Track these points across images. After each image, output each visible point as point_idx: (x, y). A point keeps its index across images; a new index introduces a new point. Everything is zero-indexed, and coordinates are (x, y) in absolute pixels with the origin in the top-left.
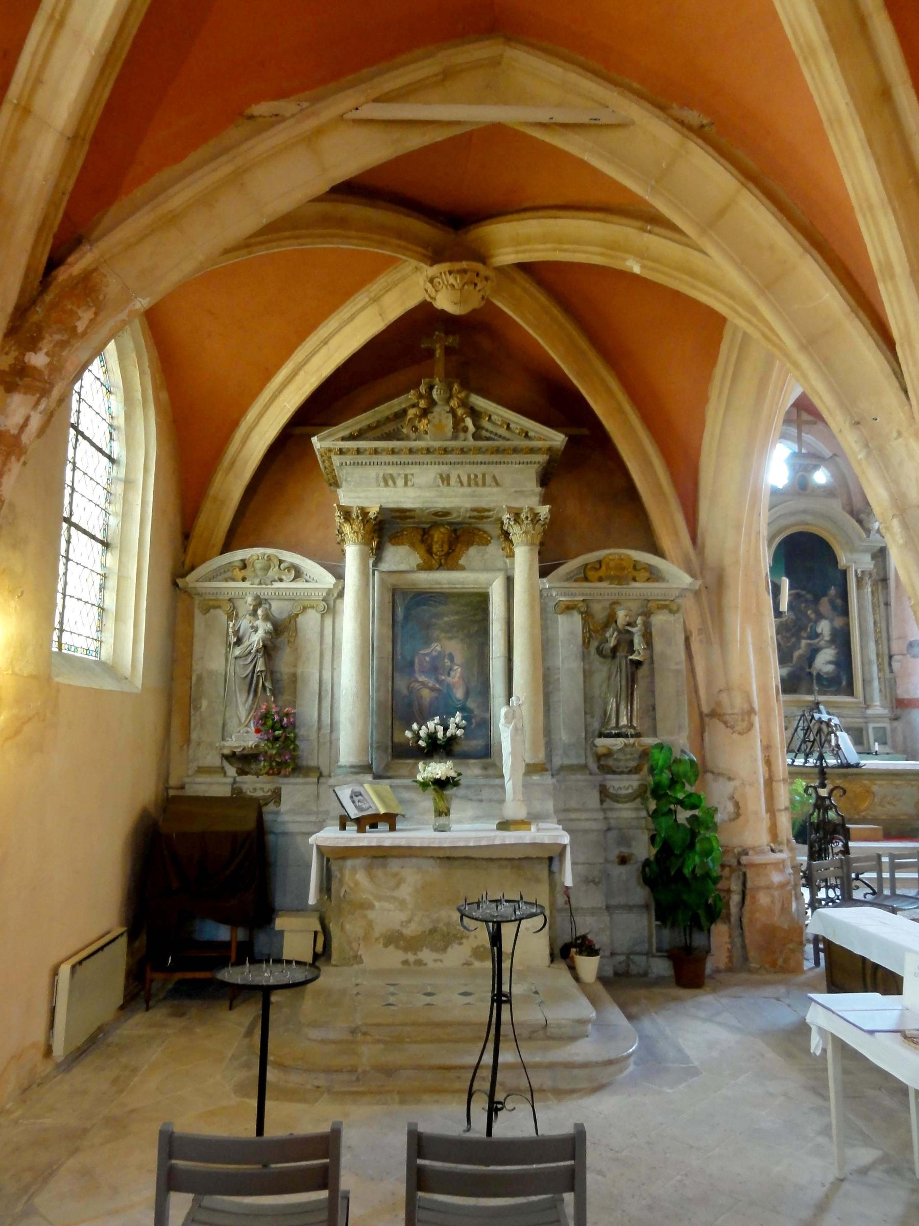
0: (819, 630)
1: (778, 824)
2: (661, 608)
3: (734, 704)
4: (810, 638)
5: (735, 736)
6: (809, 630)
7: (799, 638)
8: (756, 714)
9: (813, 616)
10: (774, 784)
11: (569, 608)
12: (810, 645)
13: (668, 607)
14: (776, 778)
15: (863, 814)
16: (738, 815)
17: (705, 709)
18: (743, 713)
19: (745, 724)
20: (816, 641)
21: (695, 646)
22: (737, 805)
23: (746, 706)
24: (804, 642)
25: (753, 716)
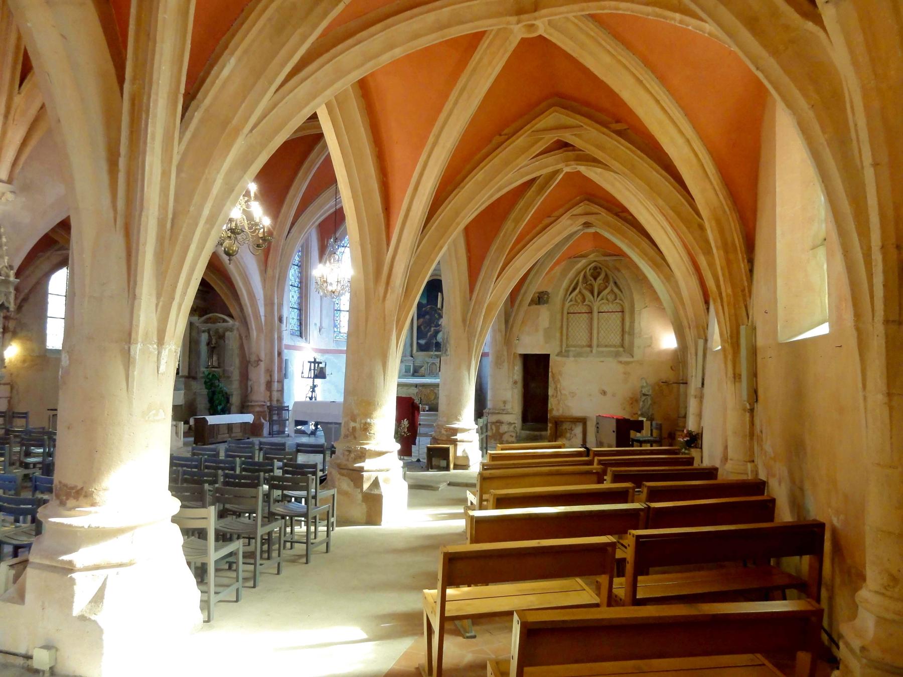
0: (440, 323)
1: (273, 396)
2: (228, 330)
3: (253, 358)
4: (436, 326)
5: (253, 368)
6: (435, 323)
7: (430, 328)
8: (261, 361)
9: (437, 317)
10: (272, 383)
11: (204, 332)
12: (435, 330)
13: (231, 329)
14: (273, 380)
15: (432, 402)
16: (251, 391)
17: (248, 359)
18: (255, 361)
19: (254, 365)
20: (438, 328)
21: (245, 341)
22: (251, 388)
23: (256, 359)
24: (432, 329)
25: (260, 362)
